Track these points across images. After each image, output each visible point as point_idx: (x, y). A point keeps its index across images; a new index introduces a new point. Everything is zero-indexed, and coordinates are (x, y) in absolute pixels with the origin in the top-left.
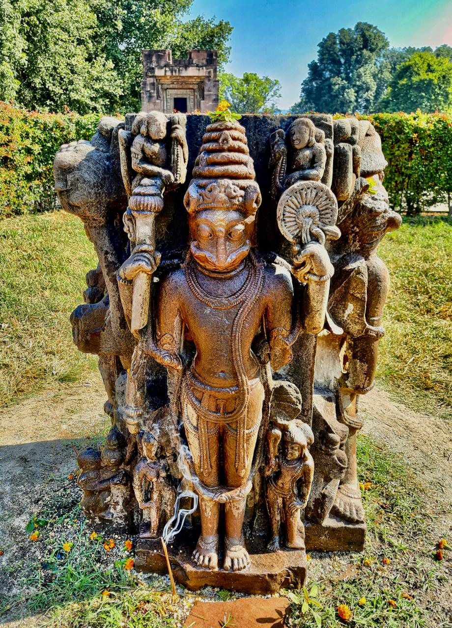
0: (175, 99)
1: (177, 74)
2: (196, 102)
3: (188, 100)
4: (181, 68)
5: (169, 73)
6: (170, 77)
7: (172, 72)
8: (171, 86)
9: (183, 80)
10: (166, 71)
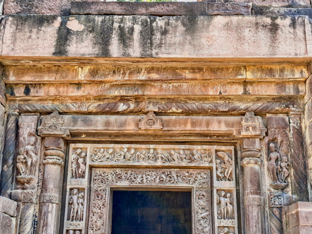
0: (118, 196)
1: (136, 50)
2: (253, 213)
3: (198, 204)
4: (160, 22)
5: (82, 47)
6: (94, 73)
7: (103, 41)
8: (99, 123)
9: (168, 89)
10: (64, 36)
